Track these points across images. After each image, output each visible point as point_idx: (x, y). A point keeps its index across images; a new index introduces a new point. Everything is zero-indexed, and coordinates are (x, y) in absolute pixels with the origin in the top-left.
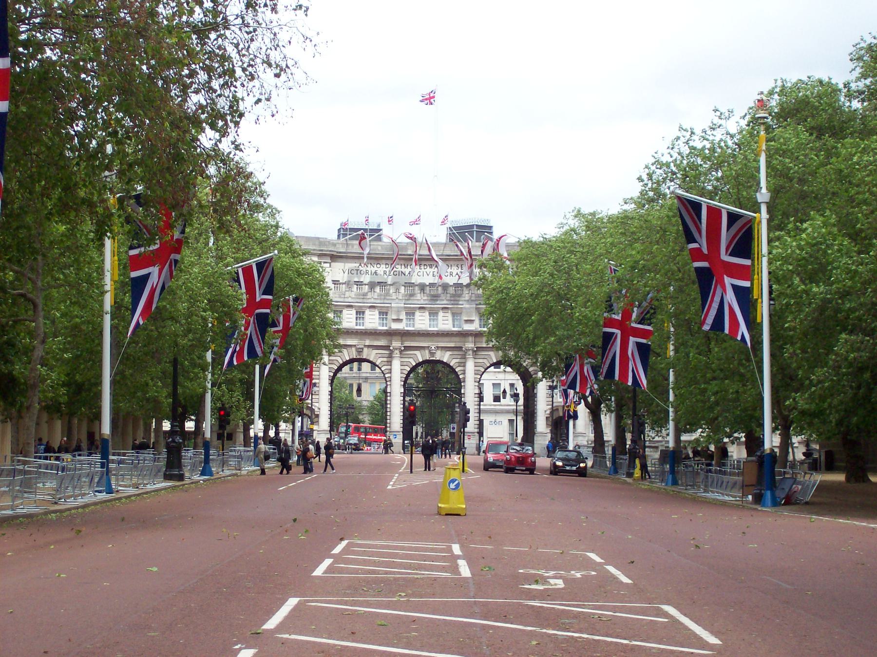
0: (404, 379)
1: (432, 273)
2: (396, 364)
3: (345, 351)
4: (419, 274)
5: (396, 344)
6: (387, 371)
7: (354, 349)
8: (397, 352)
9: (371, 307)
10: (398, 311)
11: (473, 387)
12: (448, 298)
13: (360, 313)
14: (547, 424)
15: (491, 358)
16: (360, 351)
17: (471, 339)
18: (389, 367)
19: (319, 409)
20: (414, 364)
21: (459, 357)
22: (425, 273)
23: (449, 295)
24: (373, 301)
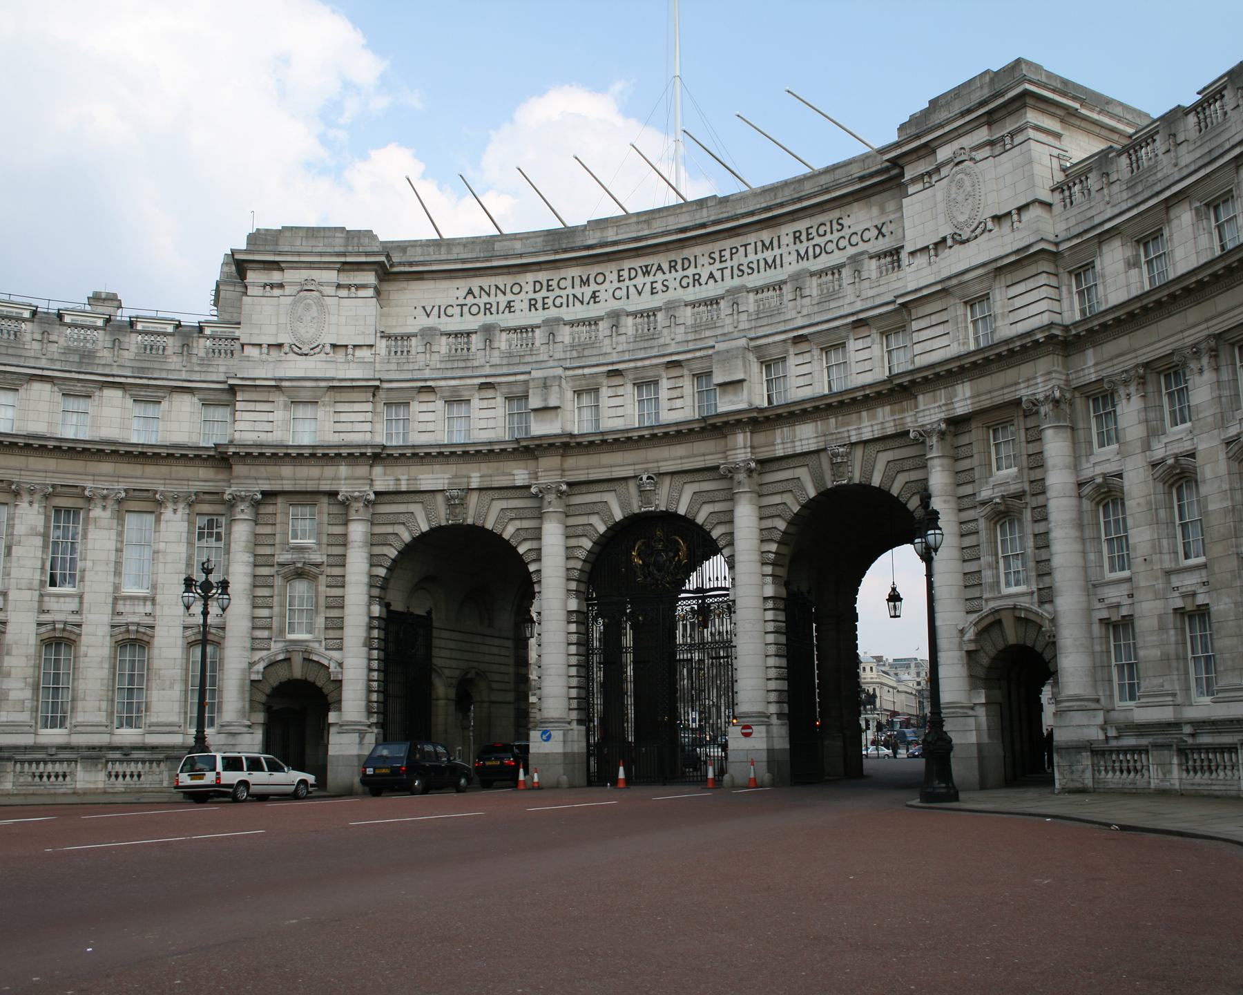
0: (576, 573)
1: (648, 287)
2: (553, 536)
3: (417, 509)
4: (618, 294)
5: (549, 472)
6: (533, 556)
7: (440, 498)
8: (550, 497)
9: (483, 386)
10: (545, 385)
11: (756, 579)
12: (679, 338)
13: (455, 400)
14: (972, 677)
15: (803, 489)
16: (456, 501)
17: (741, 439)
18: (534, 545)
19: (341, 665)
20: (602, 529)
21: (720, 495)
22: (632, 290)
23: (681, 329)
24: (487, 371)
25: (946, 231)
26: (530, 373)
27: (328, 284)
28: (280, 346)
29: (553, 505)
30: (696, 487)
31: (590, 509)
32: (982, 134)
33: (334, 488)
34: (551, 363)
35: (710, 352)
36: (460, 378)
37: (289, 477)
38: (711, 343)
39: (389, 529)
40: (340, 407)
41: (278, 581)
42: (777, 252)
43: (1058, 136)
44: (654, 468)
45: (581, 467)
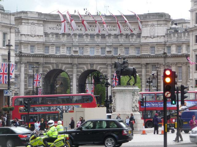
3: (51, 66)
13: (58, 48)
25: (149, 35)
26: (72, 43)
27: (36, 23)
28: (28, 35)
29: (75, 67)
30: (100, 66)
31: (81, 68)
32: (155, 23)
33: (38, 62)
34: (75, 42)
35: (105, 45)
36: (59, 43)
37: (31, 60)
38: (105, 43)
39: (45, 69)
40: (38, 47)
41: (28, 78)
42: (115, 28)
43: (166, 24)
44: (93, 62)
45: (81, 61)
